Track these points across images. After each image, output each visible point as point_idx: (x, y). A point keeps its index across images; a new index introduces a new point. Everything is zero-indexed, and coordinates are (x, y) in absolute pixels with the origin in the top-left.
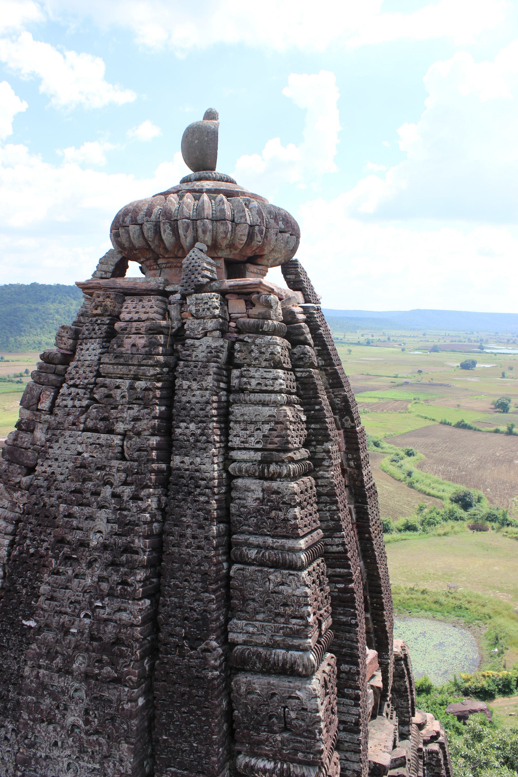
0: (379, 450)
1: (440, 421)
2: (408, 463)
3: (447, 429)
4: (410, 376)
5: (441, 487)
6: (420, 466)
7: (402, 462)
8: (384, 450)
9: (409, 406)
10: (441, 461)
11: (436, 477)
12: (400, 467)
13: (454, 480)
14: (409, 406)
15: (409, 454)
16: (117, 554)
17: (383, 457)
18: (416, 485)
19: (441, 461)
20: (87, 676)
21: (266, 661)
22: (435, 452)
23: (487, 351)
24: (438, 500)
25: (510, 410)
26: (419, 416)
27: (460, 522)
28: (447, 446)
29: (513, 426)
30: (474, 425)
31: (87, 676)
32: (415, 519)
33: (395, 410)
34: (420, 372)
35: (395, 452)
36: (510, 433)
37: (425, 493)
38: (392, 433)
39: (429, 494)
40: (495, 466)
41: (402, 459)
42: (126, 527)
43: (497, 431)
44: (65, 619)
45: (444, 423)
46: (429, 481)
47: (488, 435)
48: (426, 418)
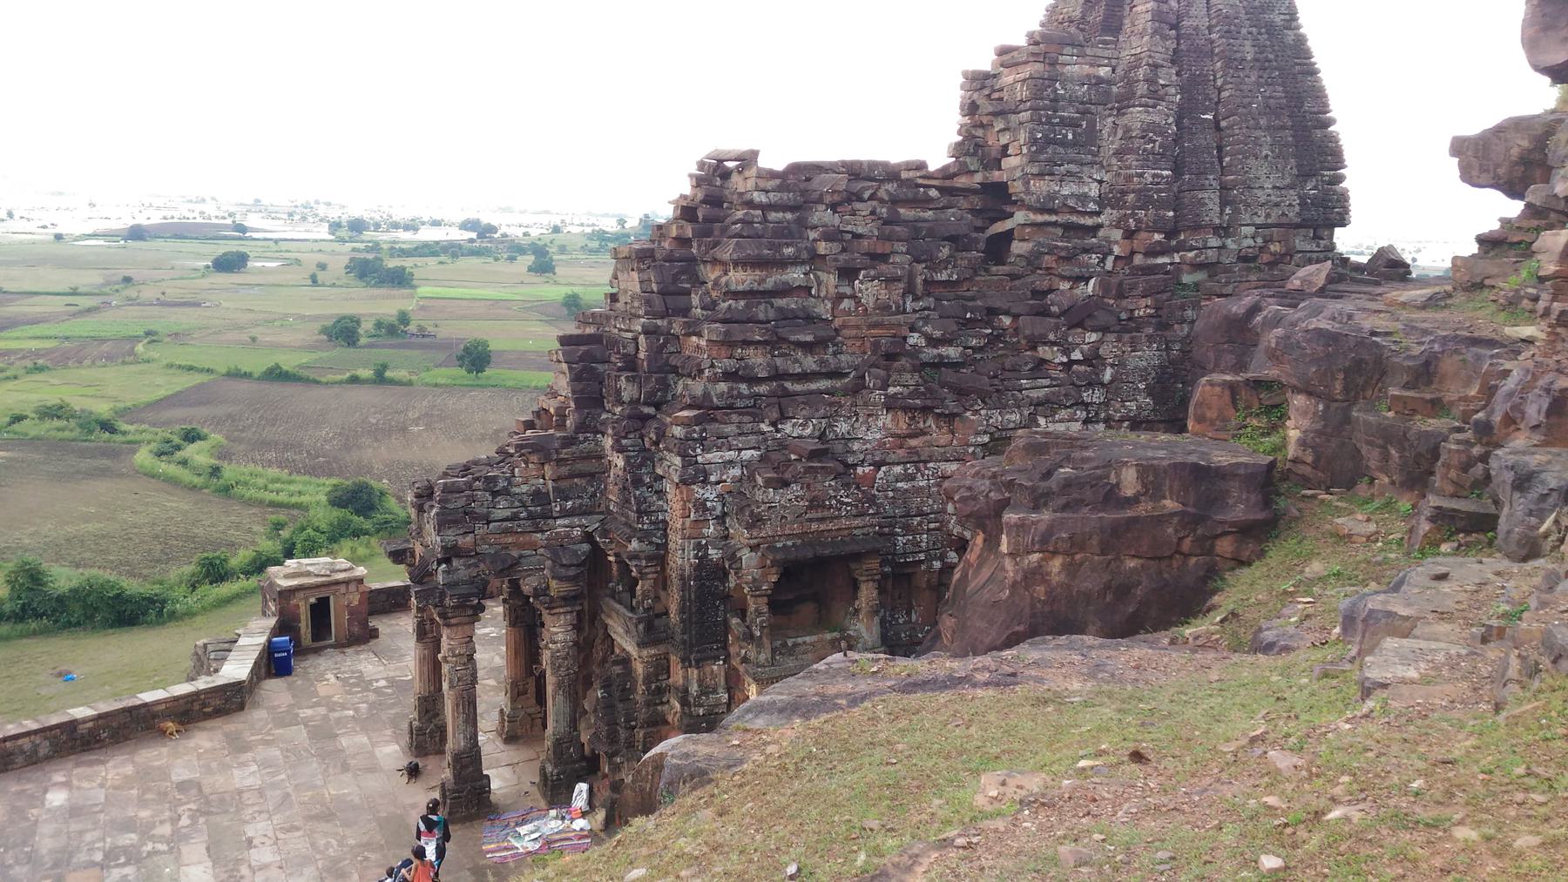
0: (118, 438)
1: (224, 371)
2: (199, 454)
3: (244, 386)
4: (107, 290)
5: (299, 487)
6: (224, 455)
7: (179, 455)
8: (130, 437)
9: (140, 348)
10: (264, 445)
11: (273, 472)
12: (184, 463)
13: (313, 471)
14: (140, 348)
15: (191, 437)
16: (1262, 64)
17: (134, 452)
18: (239, 490)
19: (264, 445)
20: (1268, 128)
21: (1318, 121)
22: (242, 431)
23: (255, 235)
24: (295, 512)
25: (363, 341)
26: (170, 366)
27: (364, 539)
28: (261, 418)
29: (385, 367)
30: (305, 373)
31: (1268, 128)
32: (268, 546)
33: (110, 358)
34: (127, 280)
35: (158, 438)
36: (380, 379)
37: (261, 503)
38: (129, 404)
39: (272, 504)
40: (377, 440)
41: (178, 448)
42: (1261, 49)
43: (355, 380)
44: (1247, 100)
45: (236, 375)
46: (261, 482)
47: (336, 389)
48: (191, 368)
